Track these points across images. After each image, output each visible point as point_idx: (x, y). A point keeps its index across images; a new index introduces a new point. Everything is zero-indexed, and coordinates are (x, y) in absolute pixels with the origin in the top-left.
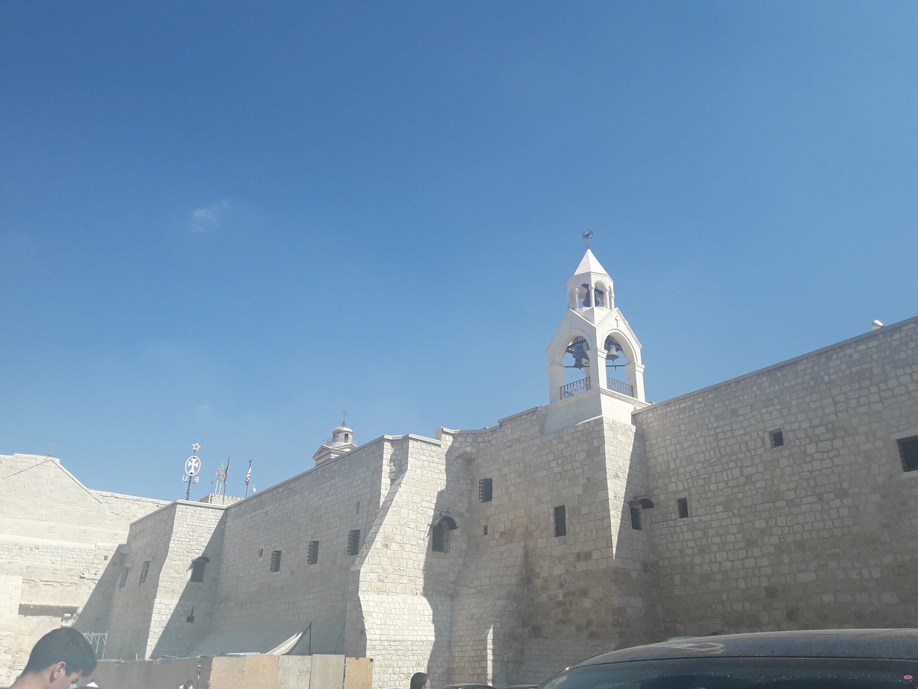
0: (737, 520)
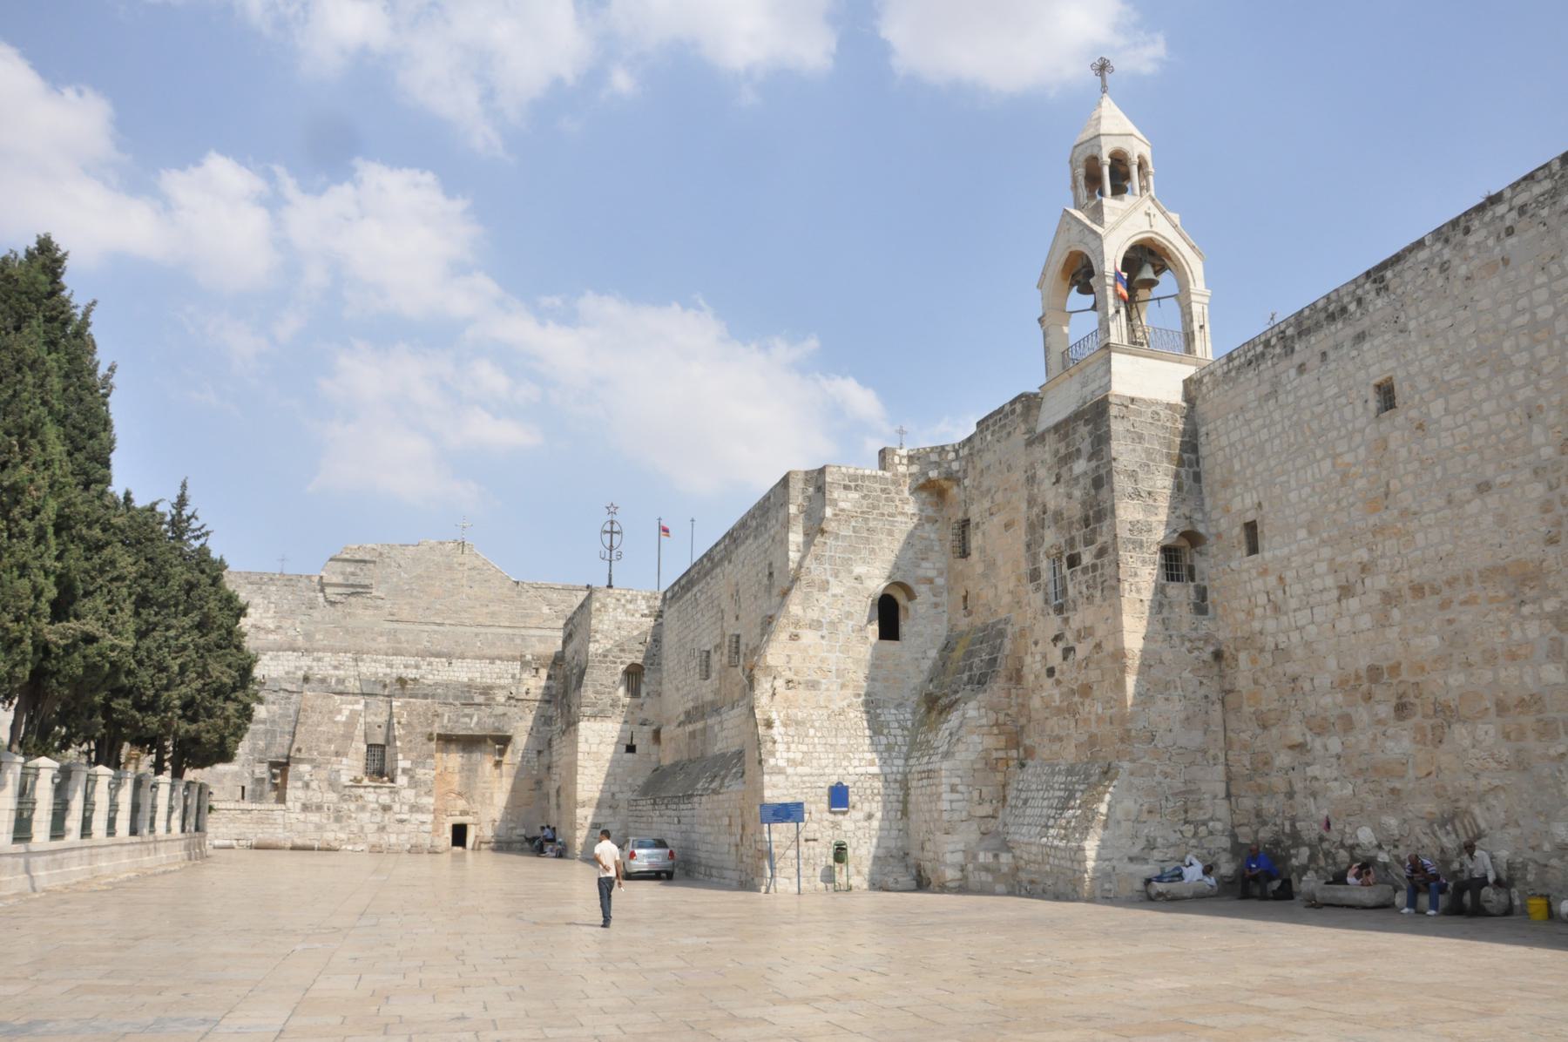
0: (1326, 552)
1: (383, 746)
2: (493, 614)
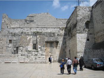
1: (36, 44)
2: (53, 24)
